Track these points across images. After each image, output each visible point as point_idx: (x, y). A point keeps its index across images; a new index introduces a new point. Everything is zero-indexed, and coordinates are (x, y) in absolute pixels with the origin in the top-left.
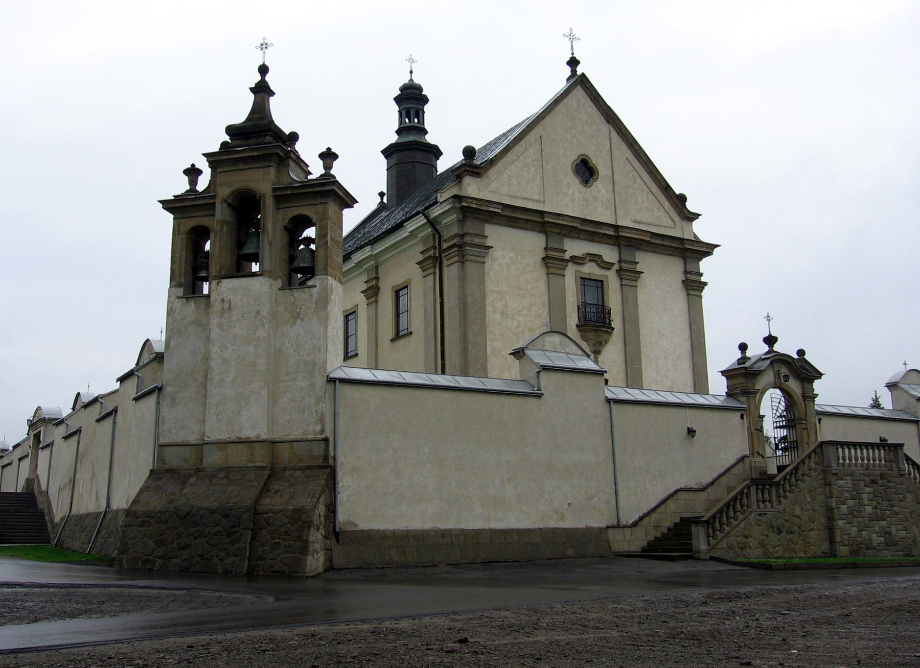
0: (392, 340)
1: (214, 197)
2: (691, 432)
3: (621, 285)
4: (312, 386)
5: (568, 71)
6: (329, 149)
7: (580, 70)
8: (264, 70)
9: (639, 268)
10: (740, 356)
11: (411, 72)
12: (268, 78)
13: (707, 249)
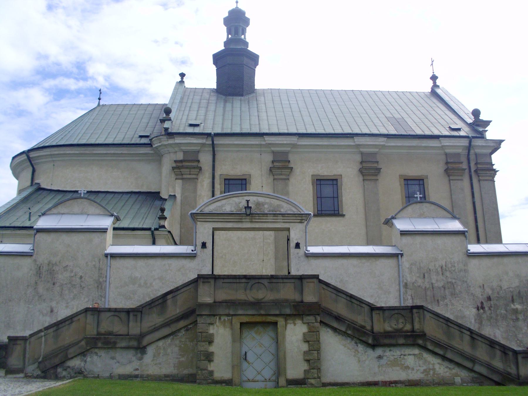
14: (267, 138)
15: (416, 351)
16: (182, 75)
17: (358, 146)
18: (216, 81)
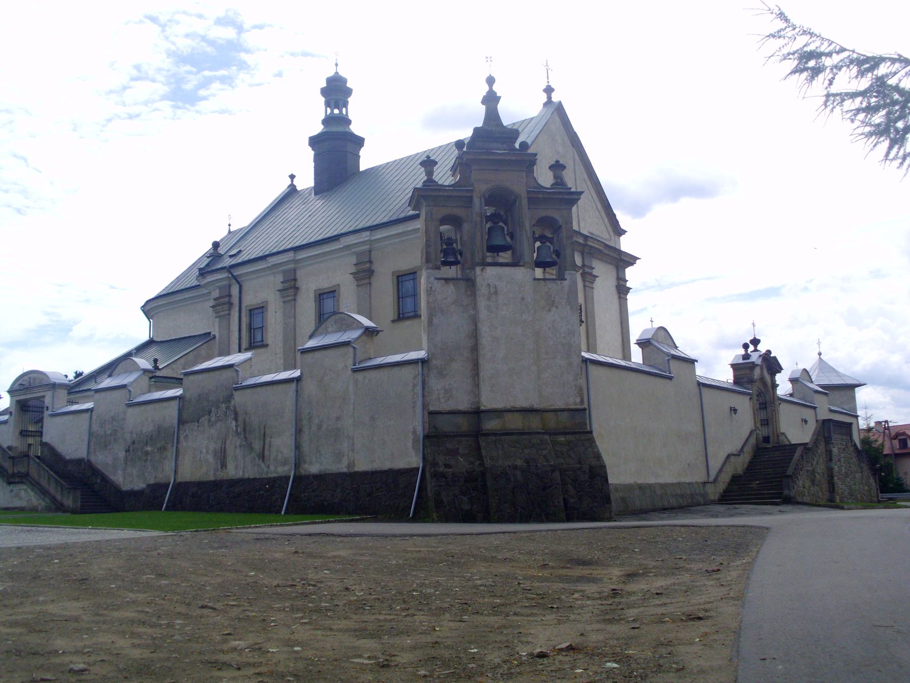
0: (393, 321)
1: (472, 191)
2: (734, 410)
3: (585, 286)
4: (570, 364)
5: (544, 97)
6: (557, 162)
8: (491, 81)
9: (595, 272)
11: (337, 65)
13: (631, 260)
15: (25, 487)
16: (292, 177)
17: (348, 247)
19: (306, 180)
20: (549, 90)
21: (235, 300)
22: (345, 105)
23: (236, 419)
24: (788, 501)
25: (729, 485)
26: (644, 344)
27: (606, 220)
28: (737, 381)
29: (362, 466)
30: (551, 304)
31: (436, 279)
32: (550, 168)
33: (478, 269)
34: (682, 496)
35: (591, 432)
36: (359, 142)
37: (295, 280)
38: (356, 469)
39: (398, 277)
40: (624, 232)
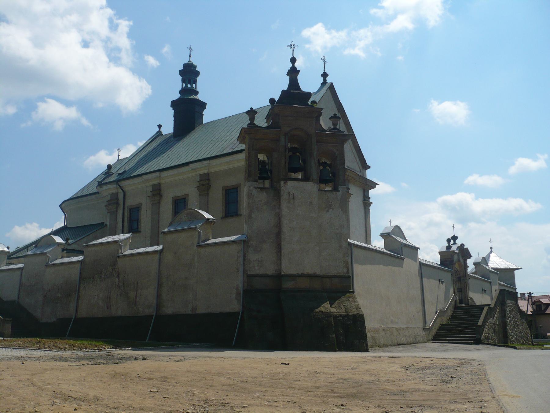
5: (321, 80)
7: (329, 80)
8: (293, 60)
10: (447, 245)
11: (190, 56)
12: (296, 65)
13: (373, 185)
14: (144, 177)
16: (160, 126)
17: (194, 170)
18: (173, 126)
19: (168, 129)
20: (325, 75)
21: (121, 202)
22: (195, 82)
23: (118, 277)
24: (478, 342)
25: (438, 330)
26: (385, 236)
27: (358, 159)
28: (443, 263)
29: (202, 310)
30: (329, 207)
31: (255, 188)
32: (330, 118)
33: (282, 183)
34: (409, 336)
35: (353, 292)
36: (203, 105)
37: (160, 190)
38: (197, 312)
39: (226, 190)
40: (369, 167)
